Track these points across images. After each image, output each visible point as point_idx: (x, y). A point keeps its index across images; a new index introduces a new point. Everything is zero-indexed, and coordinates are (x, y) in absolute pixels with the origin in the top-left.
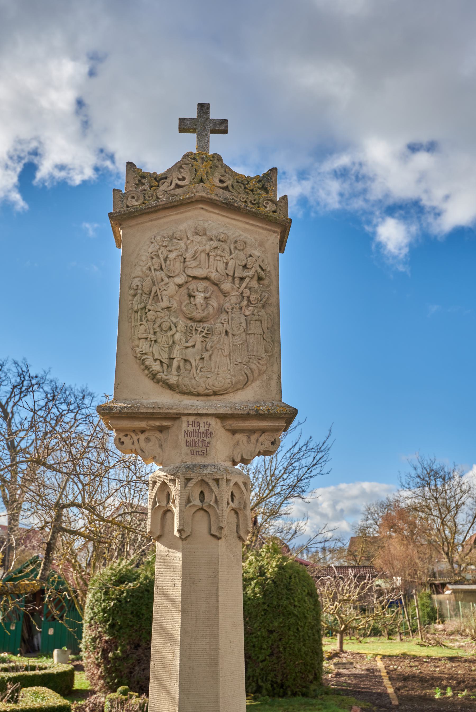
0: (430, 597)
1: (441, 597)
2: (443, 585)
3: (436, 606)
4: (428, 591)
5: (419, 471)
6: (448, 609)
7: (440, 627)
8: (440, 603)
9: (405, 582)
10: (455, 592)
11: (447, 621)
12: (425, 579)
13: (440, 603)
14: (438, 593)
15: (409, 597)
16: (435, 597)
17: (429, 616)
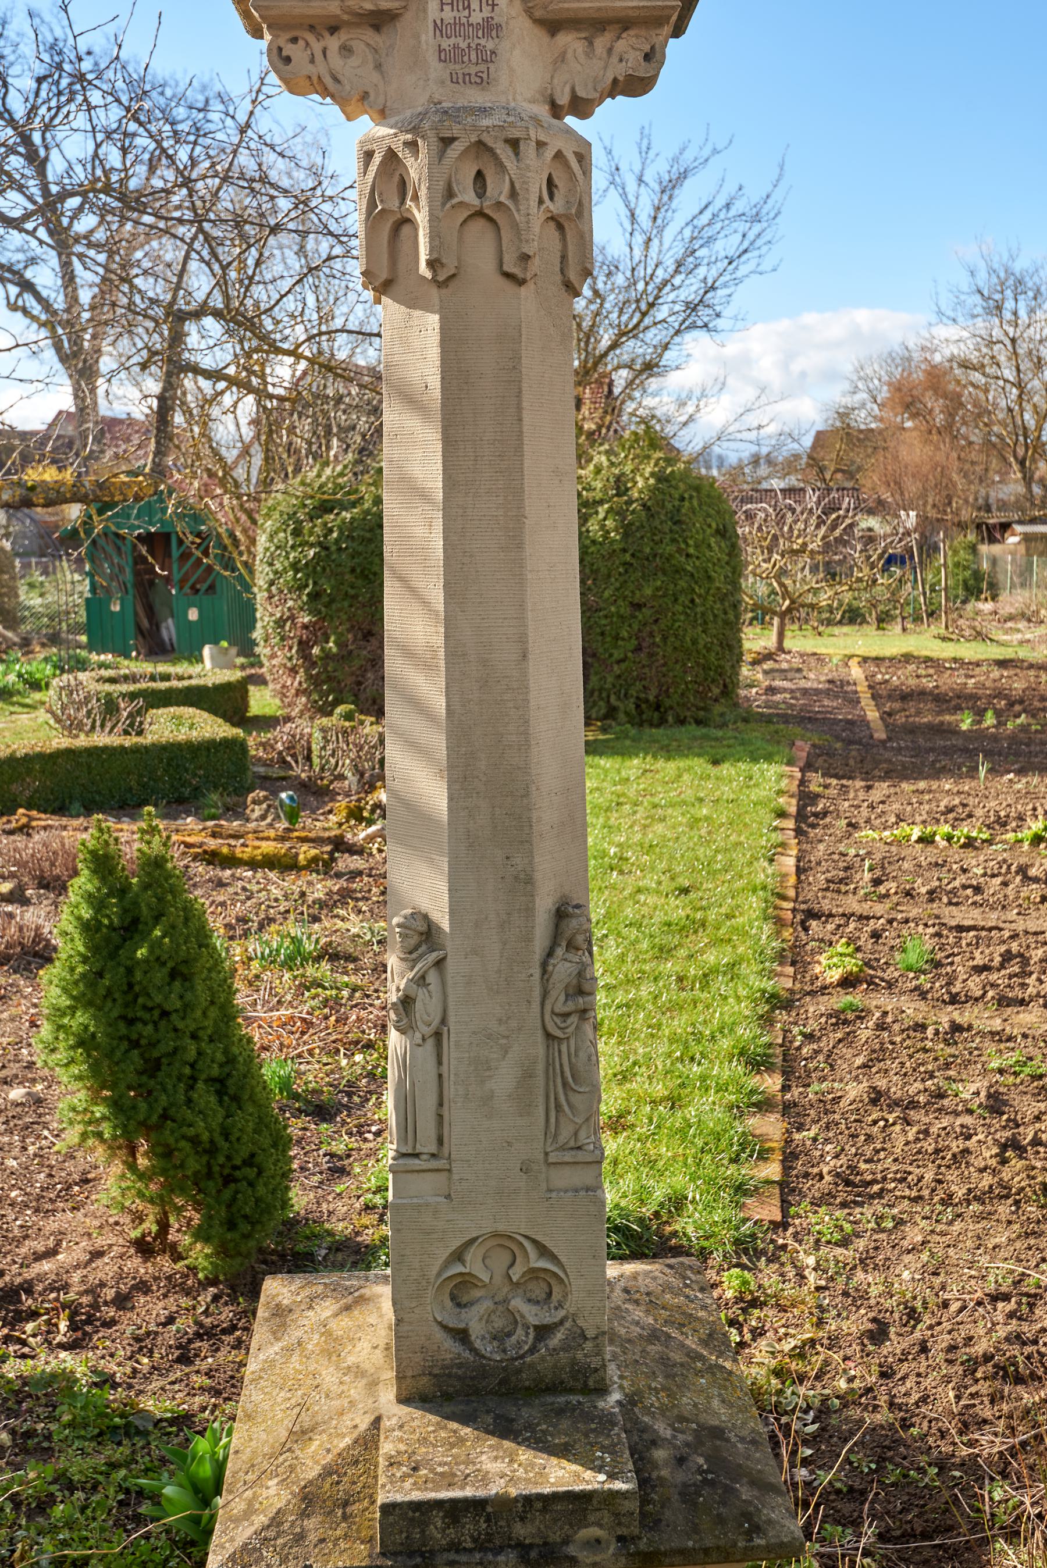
0: (973, 549)
1: (996, 549)
2: (1005, 527)
3: (985, 566)
4: (971, 537)
5: (982, 279)
6: (1008, 569)
7: (987, 607)
8: (994, 561)
9: (923, 520)
10: (1027, 538)
11: (1004, 596)
12: (966, 514)
13: (994, 561)
14: (992, 540)
15: (929, 548)
16: (984, 549)
17: (966, 587)
